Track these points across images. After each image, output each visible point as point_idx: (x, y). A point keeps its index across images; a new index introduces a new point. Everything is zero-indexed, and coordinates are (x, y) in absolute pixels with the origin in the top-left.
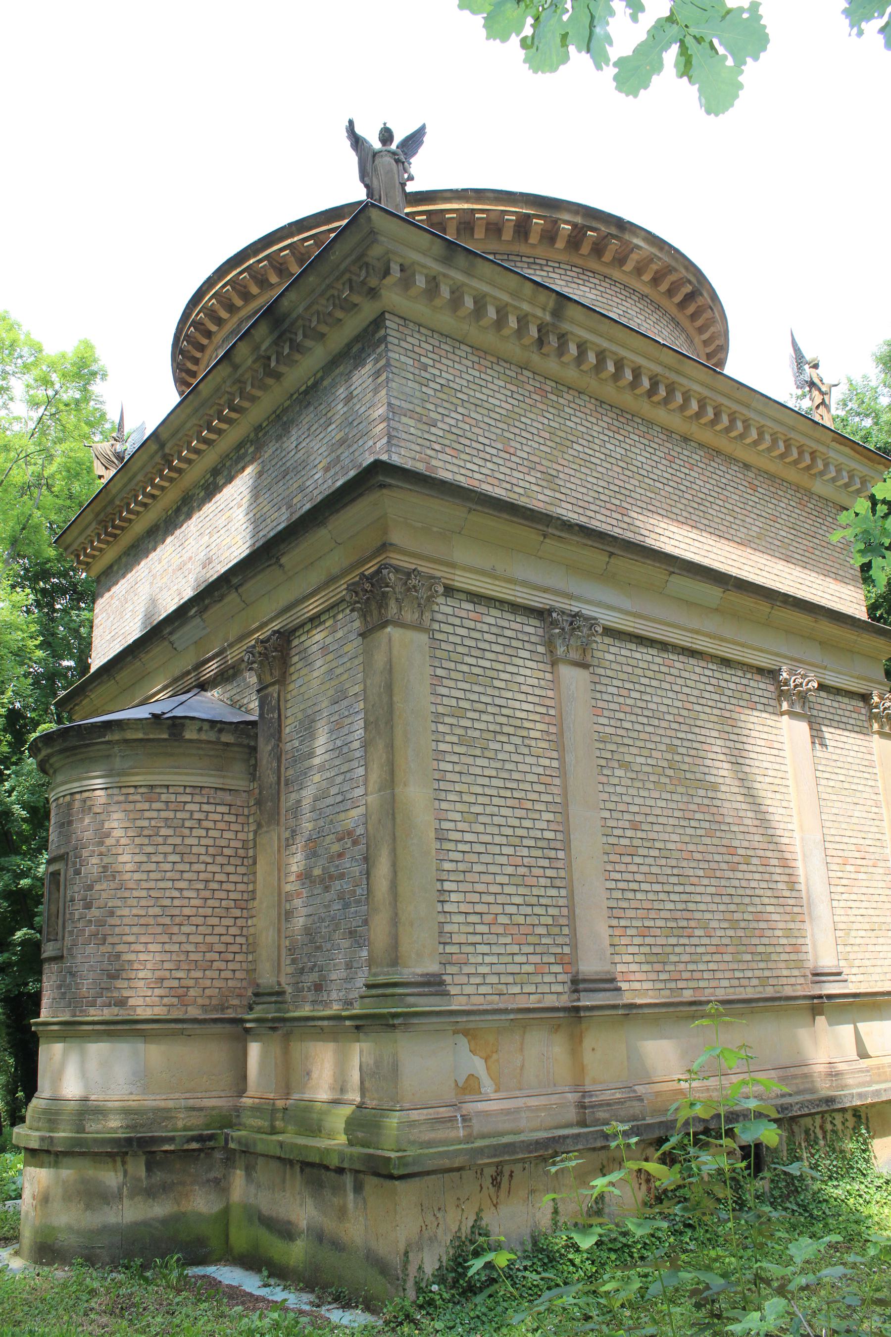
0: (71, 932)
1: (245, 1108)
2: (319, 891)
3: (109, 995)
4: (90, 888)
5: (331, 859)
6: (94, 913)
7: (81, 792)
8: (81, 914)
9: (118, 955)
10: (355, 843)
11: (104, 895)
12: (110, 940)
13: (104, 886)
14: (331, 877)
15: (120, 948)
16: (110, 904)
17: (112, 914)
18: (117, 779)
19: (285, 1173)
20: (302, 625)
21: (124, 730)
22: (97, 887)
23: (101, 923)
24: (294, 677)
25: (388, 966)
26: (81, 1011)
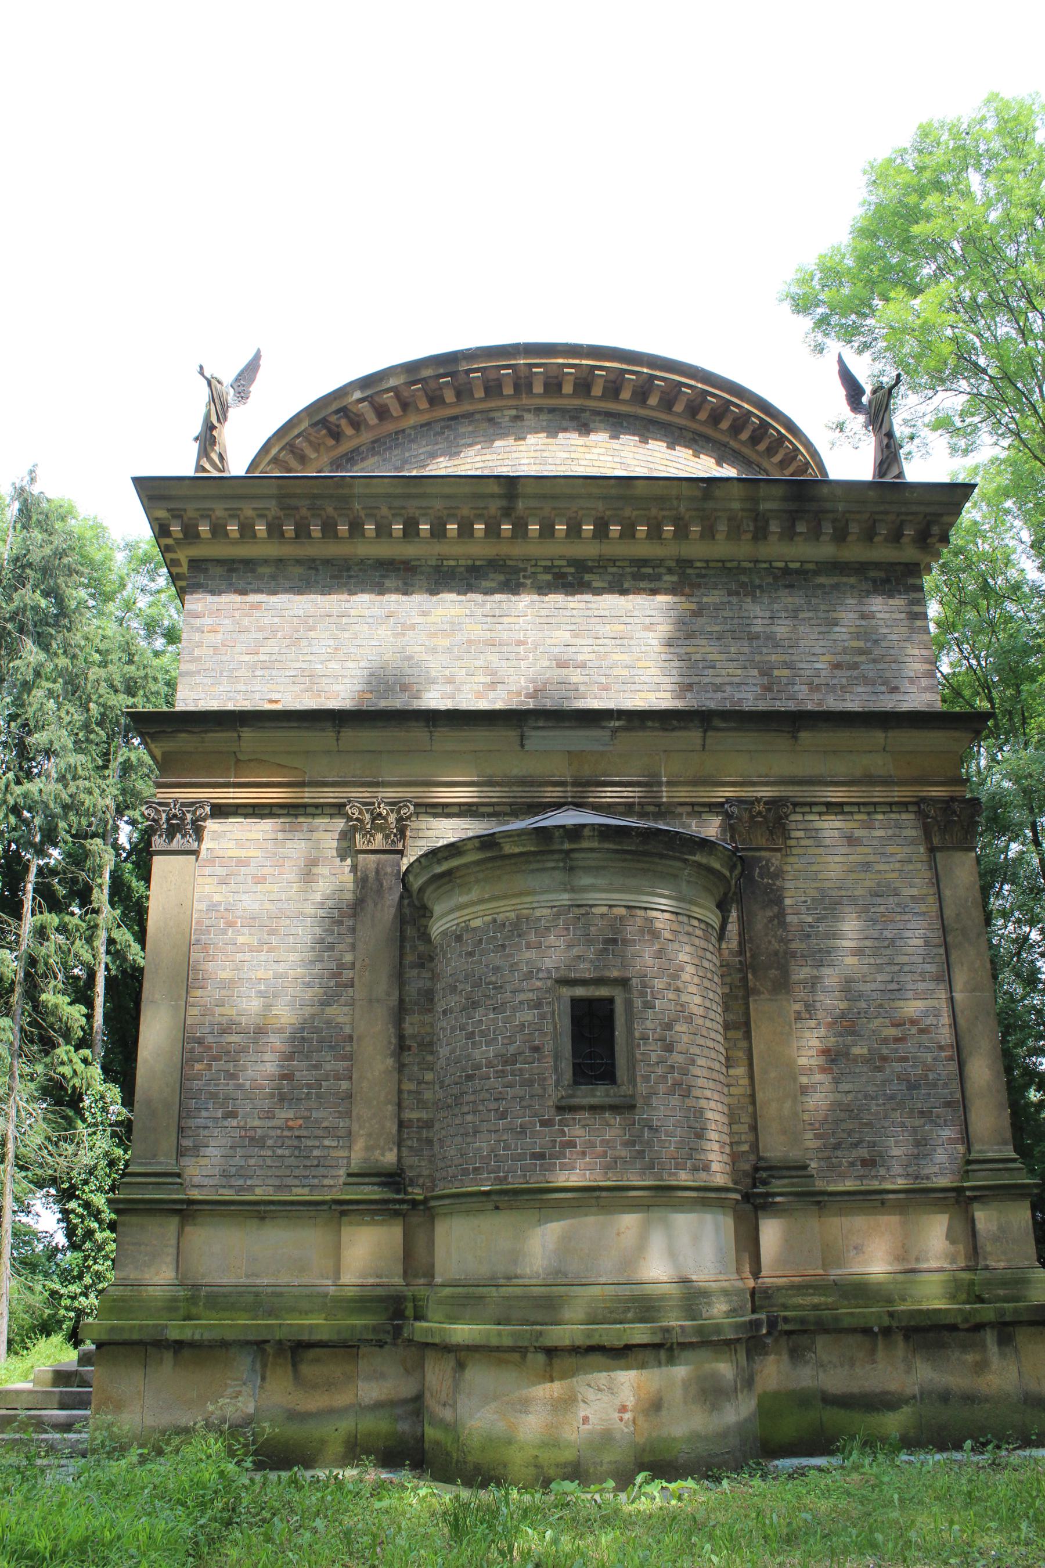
1: (779, 1288)
2: (865, 1069)
4: (669, 1027)
5: (885, 1041)
6: (677, 1058)
7: (646, 909)
8: (659, 1056)
14: (884, 1059)
16: (691, 1051)
17: (693, 1062)
18: (687, 906)
20: (811, 804)
21: (710, 854)
24: (795, 851)
25: (998, 1144)
26: (670, 1174)
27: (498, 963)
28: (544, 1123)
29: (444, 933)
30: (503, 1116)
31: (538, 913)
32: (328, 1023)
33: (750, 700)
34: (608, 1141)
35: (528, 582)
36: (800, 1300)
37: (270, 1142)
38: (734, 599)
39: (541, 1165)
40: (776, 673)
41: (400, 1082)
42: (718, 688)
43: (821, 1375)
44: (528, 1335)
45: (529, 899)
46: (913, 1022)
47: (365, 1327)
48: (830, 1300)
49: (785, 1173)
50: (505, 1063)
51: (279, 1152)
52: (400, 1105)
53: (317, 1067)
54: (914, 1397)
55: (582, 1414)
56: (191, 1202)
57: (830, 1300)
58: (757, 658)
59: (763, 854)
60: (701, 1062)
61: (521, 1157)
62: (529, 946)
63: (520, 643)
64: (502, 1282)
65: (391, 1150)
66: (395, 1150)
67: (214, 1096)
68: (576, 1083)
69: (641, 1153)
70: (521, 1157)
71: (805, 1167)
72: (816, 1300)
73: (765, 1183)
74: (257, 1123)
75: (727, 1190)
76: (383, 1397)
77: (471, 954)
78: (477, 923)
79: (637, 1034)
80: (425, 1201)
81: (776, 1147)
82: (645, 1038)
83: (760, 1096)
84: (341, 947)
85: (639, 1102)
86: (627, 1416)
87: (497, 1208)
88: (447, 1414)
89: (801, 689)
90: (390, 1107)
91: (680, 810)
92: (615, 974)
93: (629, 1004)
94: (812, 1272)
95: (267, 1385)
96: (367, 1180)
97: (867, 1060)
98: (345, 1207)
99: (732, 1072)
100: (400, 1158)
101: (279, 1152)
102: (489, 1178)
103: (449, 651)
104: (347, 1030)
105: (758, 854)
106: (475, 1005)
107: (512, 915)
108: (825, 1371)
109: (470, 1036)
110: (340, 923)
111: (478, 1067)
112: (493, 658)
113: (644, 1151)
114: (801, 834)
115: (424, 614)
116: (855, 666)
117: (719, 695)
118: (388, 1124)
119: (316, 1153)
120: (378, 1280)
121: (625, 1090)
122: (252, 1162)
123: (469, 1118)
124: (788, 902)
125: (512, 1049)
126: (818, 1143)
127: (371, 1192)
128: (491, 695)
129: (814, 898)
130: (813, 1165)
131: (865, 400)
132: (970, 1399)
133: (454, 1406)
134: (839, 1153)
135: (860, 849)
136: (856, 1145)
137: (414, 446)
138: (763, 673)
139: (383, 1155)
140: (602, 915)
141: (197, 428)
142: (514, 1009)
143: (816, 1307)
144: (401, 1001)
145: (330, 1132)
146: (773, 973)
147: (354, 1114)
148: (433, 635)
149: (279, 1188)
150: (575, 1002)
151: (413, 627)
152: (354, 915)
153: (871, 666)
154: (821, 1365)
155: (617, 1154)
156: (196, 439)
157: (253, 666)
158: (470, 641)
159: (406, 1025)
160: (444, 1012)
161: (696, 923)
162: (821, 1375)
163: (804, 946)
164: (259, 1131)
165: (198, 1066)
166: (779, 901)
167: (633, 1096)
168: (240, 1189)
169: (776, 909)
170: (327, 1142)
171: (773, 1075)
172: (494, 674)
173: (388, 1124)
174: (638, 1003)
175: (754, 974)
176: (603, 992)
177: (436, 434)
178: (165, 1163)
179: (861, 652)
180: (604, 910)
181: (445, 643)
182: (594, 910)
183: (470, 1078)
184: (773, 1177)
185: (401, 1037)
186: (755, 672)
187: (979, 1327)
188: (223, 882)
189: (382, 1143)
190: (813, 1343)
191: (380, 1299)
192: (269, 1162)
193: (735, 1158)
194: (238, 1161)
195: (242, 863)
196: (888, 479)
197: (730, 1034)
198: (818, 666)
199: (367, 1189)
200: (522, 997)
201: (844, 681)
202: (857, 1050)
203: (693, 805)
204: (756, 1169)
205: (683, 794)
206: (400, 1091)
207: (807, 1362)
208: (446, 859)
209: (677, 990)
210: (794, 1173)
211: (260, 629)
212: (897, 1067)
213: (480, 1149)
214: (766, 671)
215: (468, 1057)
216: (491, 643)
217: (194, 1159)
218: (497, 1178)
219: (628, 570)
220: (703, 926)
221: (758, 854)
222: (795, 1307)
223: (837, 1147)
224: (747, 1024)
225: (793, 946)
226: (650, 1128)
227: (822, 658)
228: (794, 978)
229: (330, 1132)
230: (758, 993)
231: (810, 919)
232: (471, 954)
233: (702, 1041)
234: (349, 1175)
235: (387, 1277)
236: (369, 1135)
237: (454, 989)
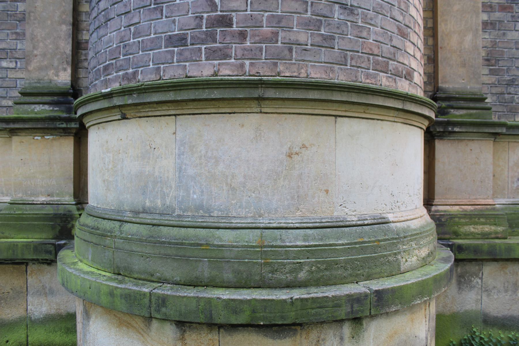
3: (401, 60)
34: (280, 19)
36: (471, 229)
39: (180, 54)
43: (485, 298)
44: (146, 301)
47: (27, 246)
48: (500, 229)
49: (462, 104)
57: (500, 229)
61: (154, 45)
64: (128, 216)
65: (65, 70)
66: (69, 70)
70: (154, 45)
71: (482, 100)
72: (487, 229)
76: (53, 312)
81: (455, 79)
83: (442, 28)
87: (124, 117)
94: (483, 202)
96: (39, 99)
98: (17, 126)
102: (118, 77)
108: (489, 295)
113: (332, 38)
120: (49, 199)
126: (493, 79)
134: (512, 90)
139: (57, 76)
143: (485, 236)
147: (28, 35)
154: (487, 291)
155: (293, 37)
162: (485, 298)
171: (456, 7)
184: (453, 108)
189: (56, 63)
190: (480, 270)
191: (46, 218)
199: (38, 108)
207: (472, 288)
210: (472, 105)
222: (467, 236)
234: (23, 94)
235: (58, 195)
236: (44, 55)
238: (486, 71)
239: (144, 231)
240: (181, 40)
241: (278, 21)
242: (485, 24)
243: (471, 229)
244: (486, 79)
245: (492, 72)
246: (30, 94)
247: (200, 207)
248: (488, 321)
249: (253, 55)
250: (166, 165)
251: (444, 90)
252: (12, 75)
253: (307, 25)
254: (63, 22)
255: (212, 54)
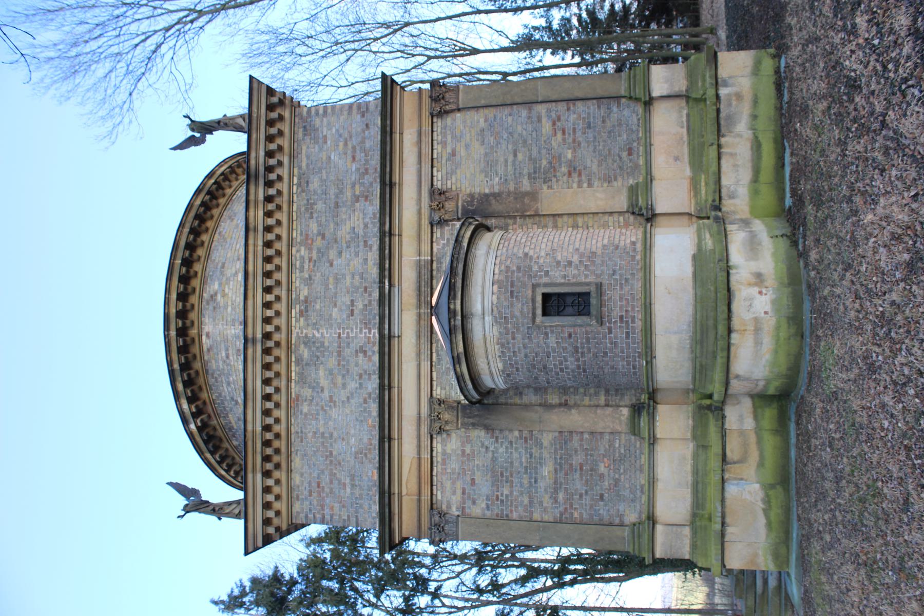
0: (586, 276)
1: (697, 203)
4: (558, 263)
5: (564, 140)
6: (575, 259)
9: (604, 246)
10: (559, 119)
11: (565, 254)
12: (594, 249)
13: (559, 254)
14: (574, 141)
15: (600, 245)
17: (577, 250)
19: (727, 153)
22: (559, 258)
23: (582, 255)
24: (459, 186)
27: (522, 355)
28: (610, 332)
29: (505, 383)
30: (605, 354)
31: (496, 333)
32: (552, 445)
33: (374, 207)
35: (304, 331)
36: (703, 192)
37: (617, 476)
38: (315, 215)
40: (357, 193)
41: (585, 406)
42: (366, 226)
45: (488, 338)
46: (554, 124)
50: (577, 352)
51: (622, 471)
52: (597, 406)
53: (576, 451)
54: (754, 134)
55: (763, 315)
56: (649, 518)
58: (349, 203)
59: (460, 204)
60: (577, 246)
61: (628, 344)
62: (514, 338)
63: (339, 337)
64: (693, 355)
67: (591, 506)
68: (588, 314)
69: (627, 280)
71: (632, 186)
72: (703, 184)
73: (641, 209)
74: (606, 483)
75: (645, 232)
77: (517, 370)
78: (500, 366)
79: (563, 281)
80: (649, 393)
81: (622, 202)
82: (564, 277)
84: (510, 437)
85: (599, 280)
86: (764, 291)
88: (761, 383)
89: (367, 179)
90: (599, 411)
91: (435, 250)
92: (530, 292)
93: (546, 285)
95: (745, 477)
97: (574, 151)
99: (580, 225)
100: (626, 406)
101: (622, 471)
103: (344, 376)
104: (557, 434)
105: (460, 208)
106: (545, 367)
107: (497, 347)
109: (562, 370)
110: (497, 438)
111: (579, 367)
112: (347, 352)
114: (449, 182)
115: (322, 390)
116: (354, 148)
117: (370, 226)
118: (607, 412)
119: (622, 451)
121: (593, 289)
122: (627, 486)
123: (606, 371)
124: (487, 191)
125: (570, 349)
126: (619, 179)
127: (644, 421)
128: (369, 353)
129: (486, 177)
130: (631, 182)
131: (198, 135)
132: (755, 102)
133: (758, 380)
135: (458, 149)
136: (621, 158)
137: (223, 394)
138: (357, 201)
140: (498, 298)
141: (213, 519)
142: (548, 347)
143: (707, 184)
144: (540, 405)
145: (611, 444)
146: (526, 200)
148: (335, 384)
149: (641, 471)
150: (545, 313)
151: (331, 397)
152: (493, 430)
153: (354, 139)
156: (220, 519)
157: (353, 486)
158: (339, 365)
159: (554, 402)
160: (548, 383)
161: (501, 246)
163: (512, 183)
164: (611, 482)
165: (576, 515)
166: (486, 195)
167: (596, 284)
168: (642, 492)
169: (491, 198)
170: (617, 445)
172: (357, 351)
173: (607, 412)
174: (545, 280)
175: (526, 211)
176: (539, 299)
177: (216, 381)
178: (626, 532)
179: (346, 144)
180: (495, 297)
181: (339, 378)
182: (495, 303)
183: (585, 371)
185: (560, 405)
186: (357, 205)
187: (718, 97)
188: (474, 503)
192: (627, 476)
193: (627, 225)
194: (626, 493)
195: (464, 493)
196: (244, 125)
197: (559, 225)
198: (354, 169)
199: (642, 424)
200: (542, 342)
201: (363, 155)
202: (569, 156)
203: (432, 242)
204: (633, 213)
205: (426, 248)
206: (590, 406)
207: (736, 190)
208: (465, 382)
209: (538, 257)
211: (331, 482)
212: (579, 134)
213: (623, 366)
214: (357, 199)
215: (573, 371)
216: (339, 353)
217: (625, 517)
218: (639, 357)
219: (298, 274)
220: (502, 241)
221: (460, 208)
223: (621, 168)
224: (554, 215)
225: (512, 189)
226: (613, 274)
227: (349, 167)
228: (528, 189)
229: (611, 444)
230: (537, 209)
231: (497, 179)
232: (517, 370)
233: (566, 244)
237: (536, 378)
238: (615, 184)
239: (698, 347)
240: (627, 333)
241: (621, 299)
242: (590, 185)
243: (703, 192)
244: (620, 183)
245: (616, 179)
246: (634, 430)
247: (689, 326)
248: (755, 180)
249: (633, 307)
250: (674, 339)
251: (629, 207)
252: (623, 442)
253: (621, 288)
254: (596, 413)
255: (633, 322)
